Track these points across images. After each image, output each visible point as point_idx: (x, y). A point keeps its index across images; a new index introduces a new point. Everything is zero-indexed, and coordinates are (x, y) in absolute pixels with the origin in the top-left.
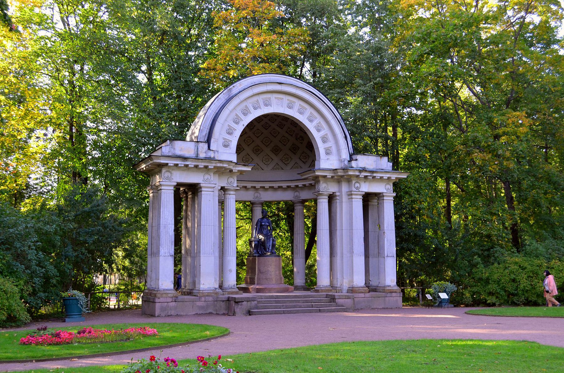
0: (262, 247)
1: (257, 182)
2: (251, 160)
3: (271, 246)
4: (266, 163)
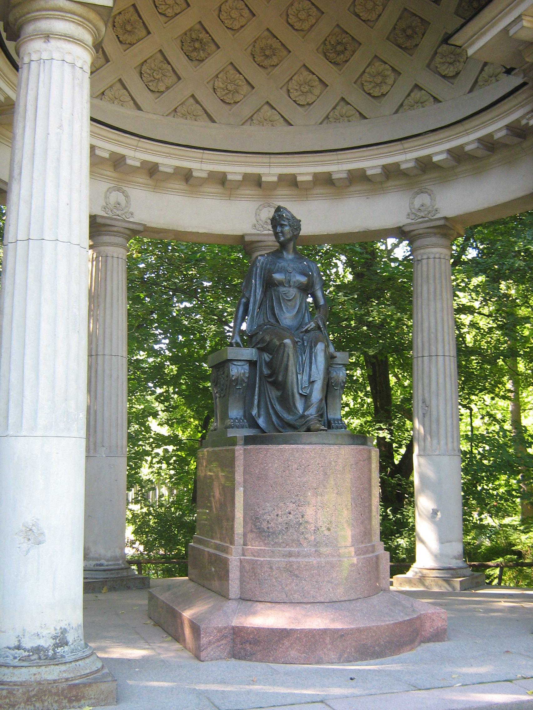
0: (274, 393)
1: (265, 159)
2: (246, 88)
3: (318, 387)
4: (302, 100)
